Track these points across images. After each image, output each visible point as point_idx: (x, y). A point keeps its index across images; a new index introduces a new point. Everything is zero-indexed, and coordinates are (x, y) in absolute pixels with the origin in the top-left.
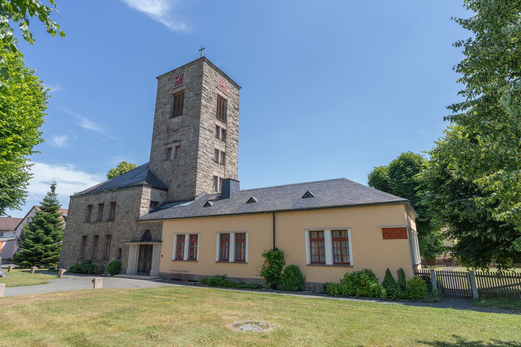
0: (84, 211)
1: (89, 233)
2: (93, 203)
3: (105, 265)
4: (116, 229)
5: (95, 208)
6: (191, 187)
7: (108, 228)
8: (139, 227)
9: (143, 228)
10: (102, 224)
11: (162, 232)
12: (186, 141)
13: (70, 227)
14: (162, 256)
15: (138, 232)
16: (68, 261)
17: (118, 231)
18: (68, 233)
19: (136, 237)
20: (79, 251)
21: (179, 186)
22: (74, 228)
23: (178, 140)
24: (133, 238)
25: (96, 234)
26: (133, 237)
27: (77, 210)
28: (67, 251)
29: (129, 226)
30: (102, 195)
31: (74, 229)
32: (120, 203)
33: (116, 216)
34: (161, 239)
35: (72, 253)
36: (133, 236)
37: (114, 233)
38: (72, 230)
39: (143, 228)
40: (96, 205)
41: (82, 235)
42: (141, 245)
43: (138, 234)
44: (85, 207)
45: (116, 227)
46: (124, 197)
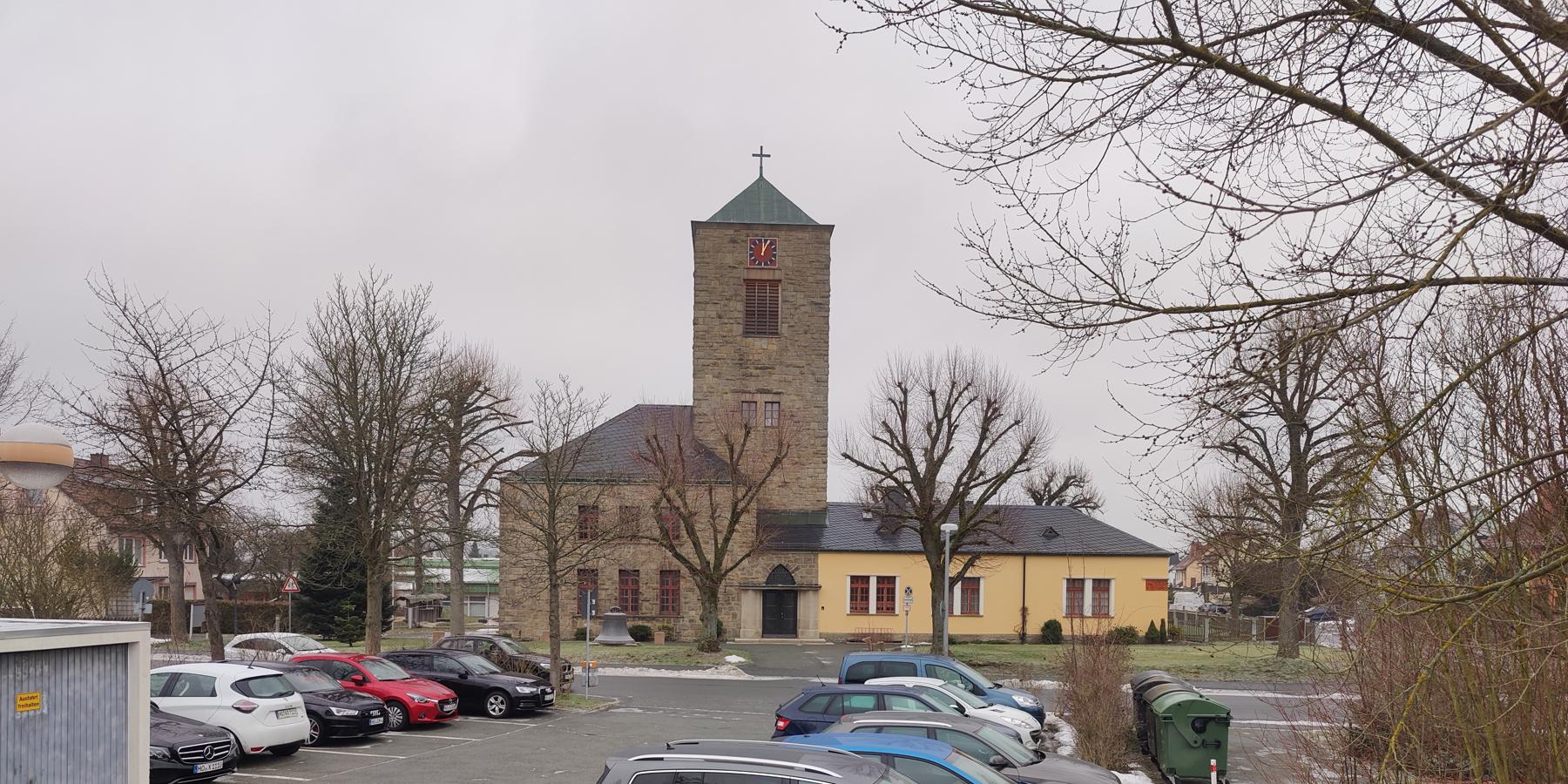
3: (671, 625)
12: (793, 397)
23: (775, 391)
42: (764, 591)
43: (757, 572)
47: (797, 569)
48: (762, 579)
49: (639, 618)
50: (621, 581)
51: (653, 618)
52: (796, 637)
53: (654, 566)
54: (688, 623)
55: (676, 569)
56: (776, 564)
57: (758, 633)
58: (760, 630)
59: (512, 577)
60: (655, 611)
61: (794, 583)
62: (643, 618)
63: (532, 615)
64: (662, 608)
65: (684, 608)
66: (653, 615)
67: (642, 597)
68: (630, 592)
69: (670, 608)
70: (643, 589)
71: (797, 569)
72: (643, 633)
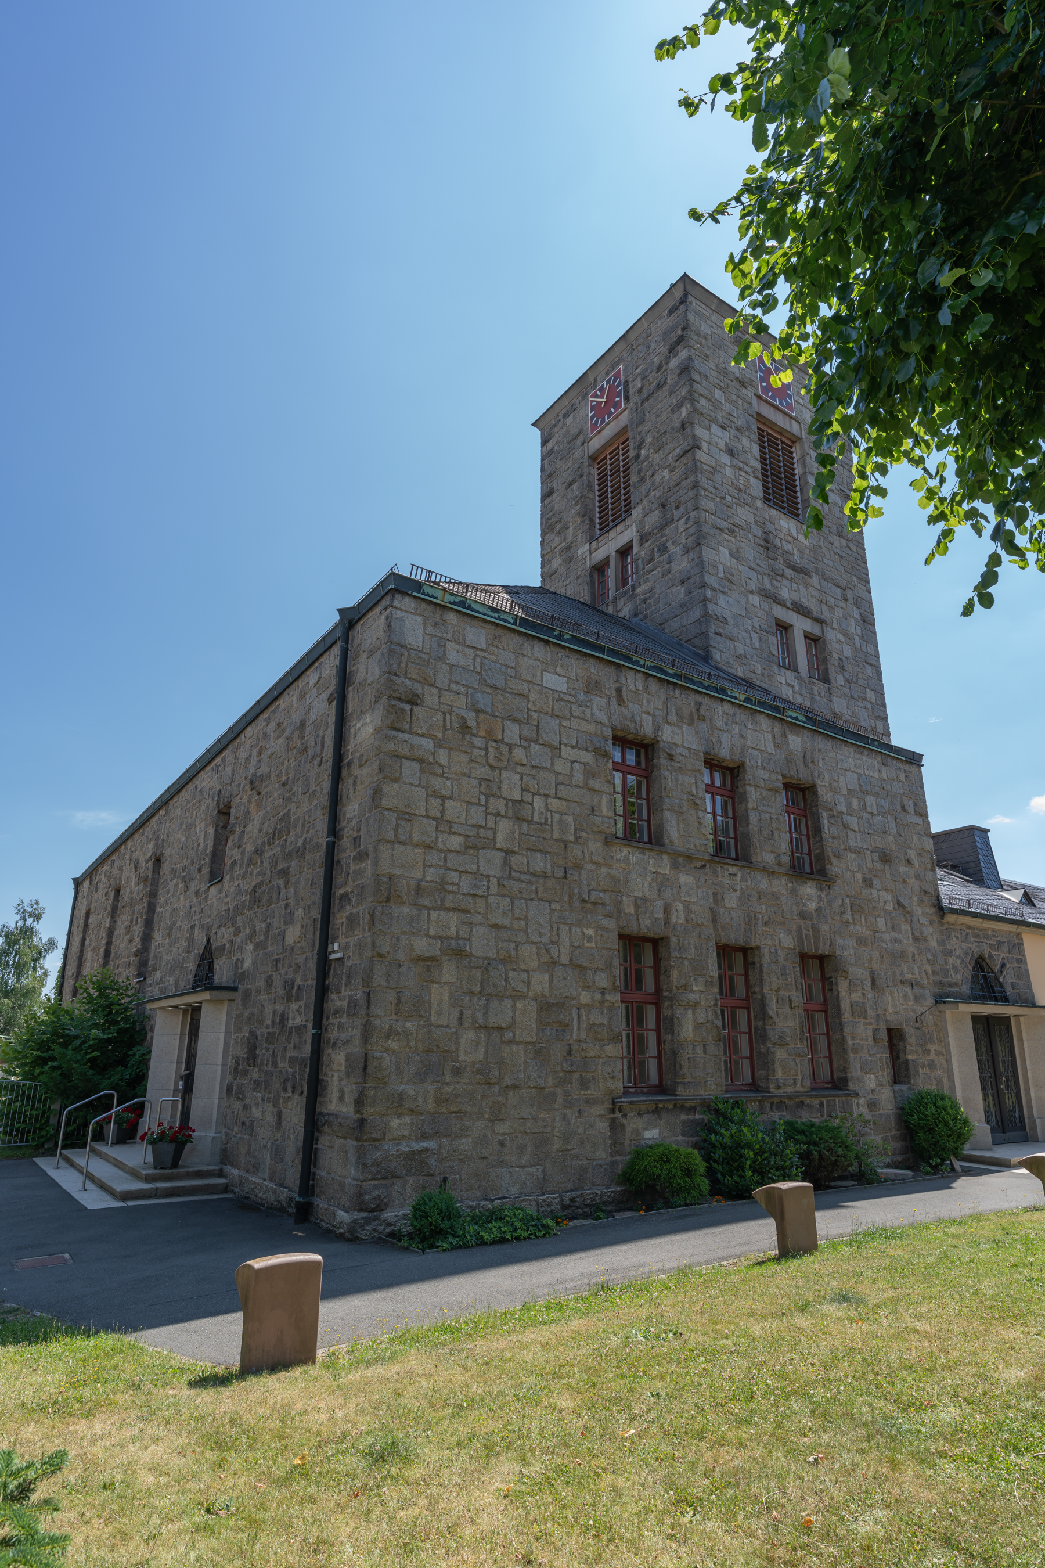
0: (588, 757)
1: (678, 917)
2: (657, 728)
7: (803, 915)
10: (763, 883)
13: (455, 842)
16: (500, 1128)
22: (508, 852)
25: (736, 938)
27: (515, 728)
28: (468, 1036)
31: (506, 863)
35: (540, 1054)
37: (842, 947)
38: (495, 871)
40: (685, 752)
41: (610, 924)
44: (591, 728)
59: (421, 945)
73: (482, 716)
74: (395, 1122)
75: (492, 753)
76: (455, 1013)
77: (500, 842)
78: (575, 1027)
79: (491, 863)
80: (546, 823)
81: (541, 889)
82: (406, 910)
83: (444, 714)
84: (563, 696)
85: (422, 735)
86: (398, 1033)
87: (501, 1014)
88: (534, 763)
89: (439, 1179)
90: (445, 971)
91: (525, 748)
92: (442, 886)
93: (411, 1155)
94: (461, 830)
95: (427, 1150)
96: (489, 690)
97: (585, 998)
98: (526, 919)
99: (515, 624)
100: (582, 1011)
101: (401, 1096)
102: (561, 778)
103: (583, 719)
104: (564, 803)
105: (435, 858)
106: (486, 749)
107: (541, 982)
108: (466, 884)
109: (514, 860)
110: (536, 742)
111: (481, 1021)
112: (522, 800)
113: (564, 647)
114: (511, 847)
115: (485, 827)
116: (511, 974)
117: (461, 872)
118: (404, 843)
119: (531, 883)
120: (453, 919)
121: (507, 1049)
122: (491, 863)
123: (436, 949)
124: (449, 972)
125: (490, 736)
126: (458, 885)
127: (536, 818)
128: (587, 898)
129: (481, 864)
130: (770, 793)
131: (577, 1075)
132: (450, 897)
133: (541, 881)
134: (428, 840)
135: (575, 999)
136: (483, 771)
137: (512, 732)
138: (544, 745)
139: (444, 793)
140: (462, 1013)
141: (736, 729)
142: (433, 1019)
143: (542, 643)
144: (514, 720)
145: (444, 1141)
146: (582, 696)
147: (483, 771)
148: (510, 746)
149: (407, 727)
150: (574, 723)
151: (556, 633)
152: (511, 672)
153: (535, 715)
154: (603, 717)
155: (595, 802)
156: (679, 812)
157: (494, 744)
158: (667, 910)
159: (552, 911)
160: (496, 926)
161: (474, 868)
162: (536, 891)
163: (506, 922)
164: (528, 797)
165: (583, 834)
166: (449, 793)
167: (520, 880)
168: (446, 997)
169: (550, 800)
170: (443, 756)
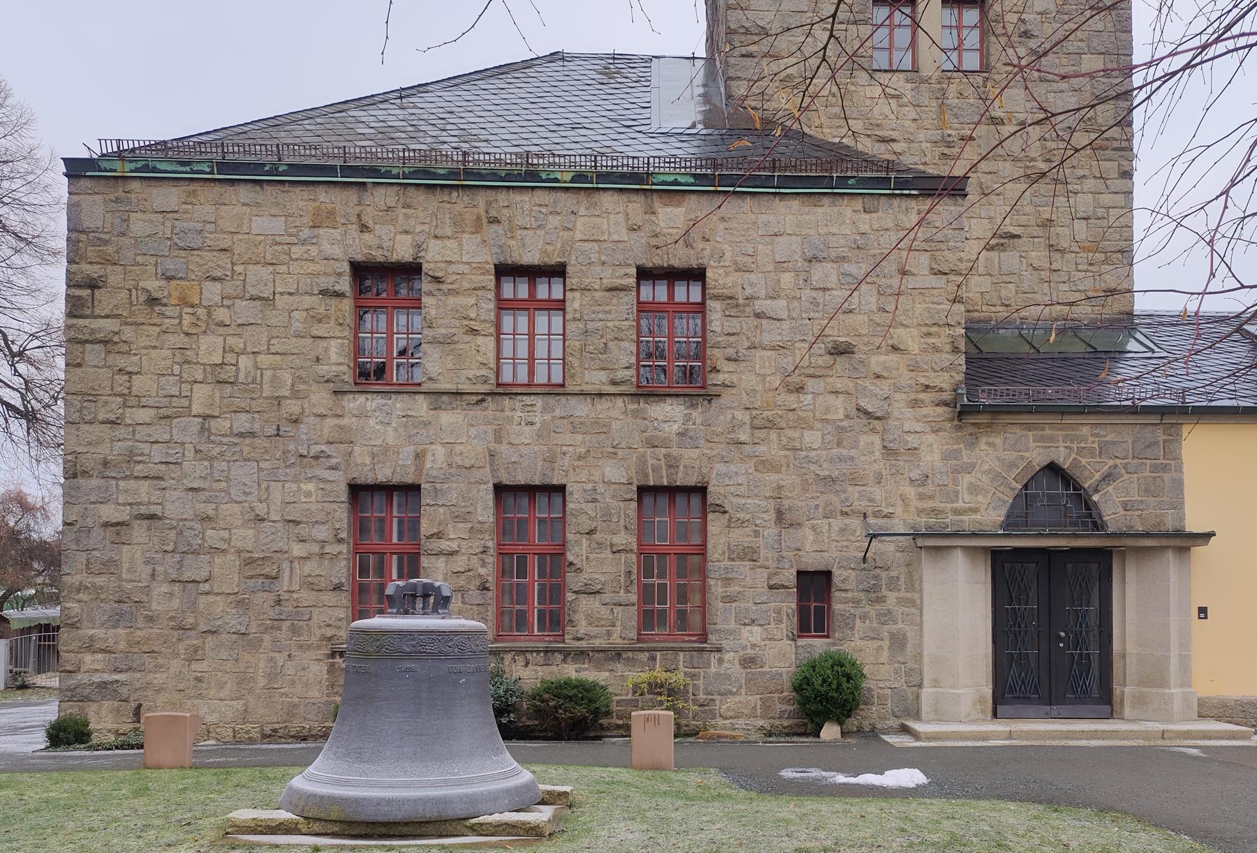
3: (678, 678)
4: (748, 448)
5: (455, 293)
6: (1100, 257)
8: (972, 445)
9: (1011, 456)
11: (1179, 485)
14: (1203, 611)
15: (966, 479)
17: (764, 465)
18: (131, 452)
19: (960, 504)
20: (337, 588)
21: (1003, 240)
22: (206, 417)
24: (935, 511)
26: (929, 504)
29: (876, 439)
30: (524, 205)
32: (756, 283)
33: (725, 366)
34: (1182, 519)
36: (921, 497)
39: (1011, 456)
43: (974, 489)
45: (743, 437)
46: (788, 247)
47: (1108, 478)
48: (990, 513)
49: (567, 654)
50: (503, 527)
51: (616, 654)
52: (1110, 716)
53: (614, 472)
54: (736, 670)
55: (692, 481)
56: (1038, 458)
57: (981, 701)
58: (988, 691)
59: (109, 512)
60: (624, 625)
61: (1097, 525)
62: (581, 655)
63: (181, 647)
64: (648, 619)
65: (723, 618)
66: (616, 640)
67: (573, 581)
68: (534, 564)
69: (672, 616)
70: (577, 551)
71: (1108, 478)
72: (580, 711)
73: (174, 282)
74: (88, 658)
75: (187, 320)
76: (149, 569)
77: (196, 409)
78: (286, 579)
79: (186, 430)
80: (254, 382)
81: (246, 449)
82: (94, 482)
83: (130, 290)
84: (277, 238)
85: (107, 317)
86: (87, 588)
87: (196, 568)
88: (239, 321)
89: (134, 705)
90: (135, 534)
91: (228, 307)
92: (131, 457)
93: (103, 685)
94: (151, 402)
95: (117, 681)
96: (182, 253)
97: (297, 550)
98: (228, 479)
99: (212, 173)
100: (296, 564)
101: (92, 639)
102: (275, 332)
103: (307, 260)
104: (278, 357)
105: (122, 432)
106: (181, 317)
107: (245, 537)
108: (157, 453)
109: (214, 425)
110: (242, 298)
111: (174, 576)
112: (223, 363)
113: (283, 182)
114: (209, 412)
115: (180, 396)
116: (209, 532)
117: (152, 443)
118: (90, 423)
119: (236, 444)
120: (144, 486)
121: (203, 599)
122: (186, 430)
123: (123, 515)
124: (139, 532)
125: (184, 302)
126: (149, 455)
127: (242, 378)
128: (305, 452)
129: (175, 431)
130: (607, 294)
131: (288, 623)
132: (140, 467)
133: (248, 441)
134: (112, 417)
135: (286, 552)
136: (178, 340)
137: (213, 292)
138: (252, 298)
139: (129, 369)
140: (154, 570)
141: (554, 221)
142: (124, 576)
143: (249, 186)
144: (215, 279)
145: (138, 675)
146: (306, 233)
147: (178, 340)
148: (209, 309)
149: (88, 312)
150: (294, 267)
151: (267, 168)
152: (210, 227)
153: (239, 269)
154: (337, 251)
155: (320, 351)
156: (446, 342)
157: (190, 310)
158: (419, 456)
159: (260, 470)
160: (192, 489)
161: (166, 437)
162: (241, 451)
163: (206, 485)
164: (230, 358)
165: (302, 387)
166: (136, 369)
167: (221, 443)
168: (138, 554)
169: (260, 358)
170: (128, 333)
